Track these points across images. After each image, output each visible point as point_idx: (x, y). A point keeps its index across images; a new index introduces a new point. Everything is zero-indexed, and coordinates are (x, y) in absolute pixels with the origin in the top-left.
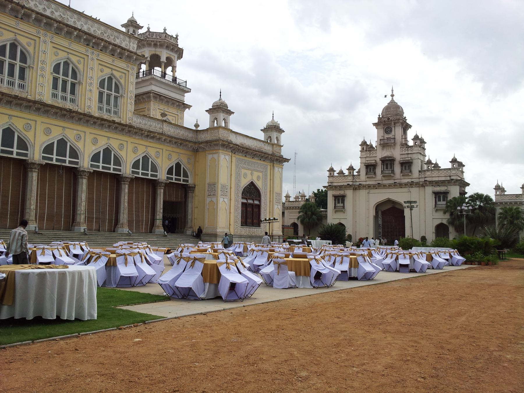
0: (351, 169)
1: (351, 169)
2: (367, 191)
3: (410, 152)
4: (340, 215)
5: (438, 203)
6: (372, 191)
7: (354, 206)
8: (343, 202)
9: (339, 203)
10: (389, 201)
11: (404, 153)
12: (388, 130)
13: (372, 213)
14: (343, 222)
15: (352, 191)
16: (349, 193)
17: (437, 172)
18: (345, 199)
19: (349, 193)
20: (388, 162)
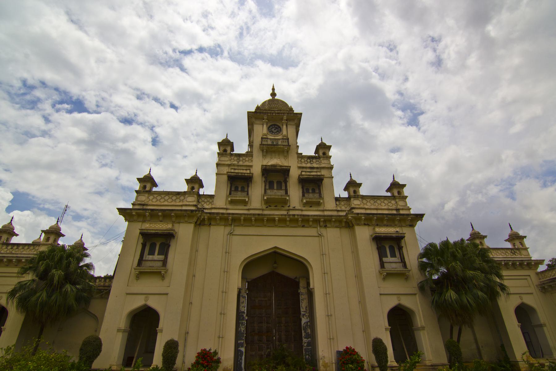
0: (195, 182)
1: (195, 182)
2: (228, 229)
3: (315, 165)
4: (150, 285)
5: (385, 259)
6: (239, 230)
7: (192, 263)
8: (165, 250)
9: (152, 253)
10: (275, 255)
11: (304, 165)
12: (275, 128)
13: (236, 281)
14: (153, 303)
15: (192, 226)
16: (185, 231)
17: (372, 202)
18: (173, 244)
19: (185, 231)
20: (276, 177)
